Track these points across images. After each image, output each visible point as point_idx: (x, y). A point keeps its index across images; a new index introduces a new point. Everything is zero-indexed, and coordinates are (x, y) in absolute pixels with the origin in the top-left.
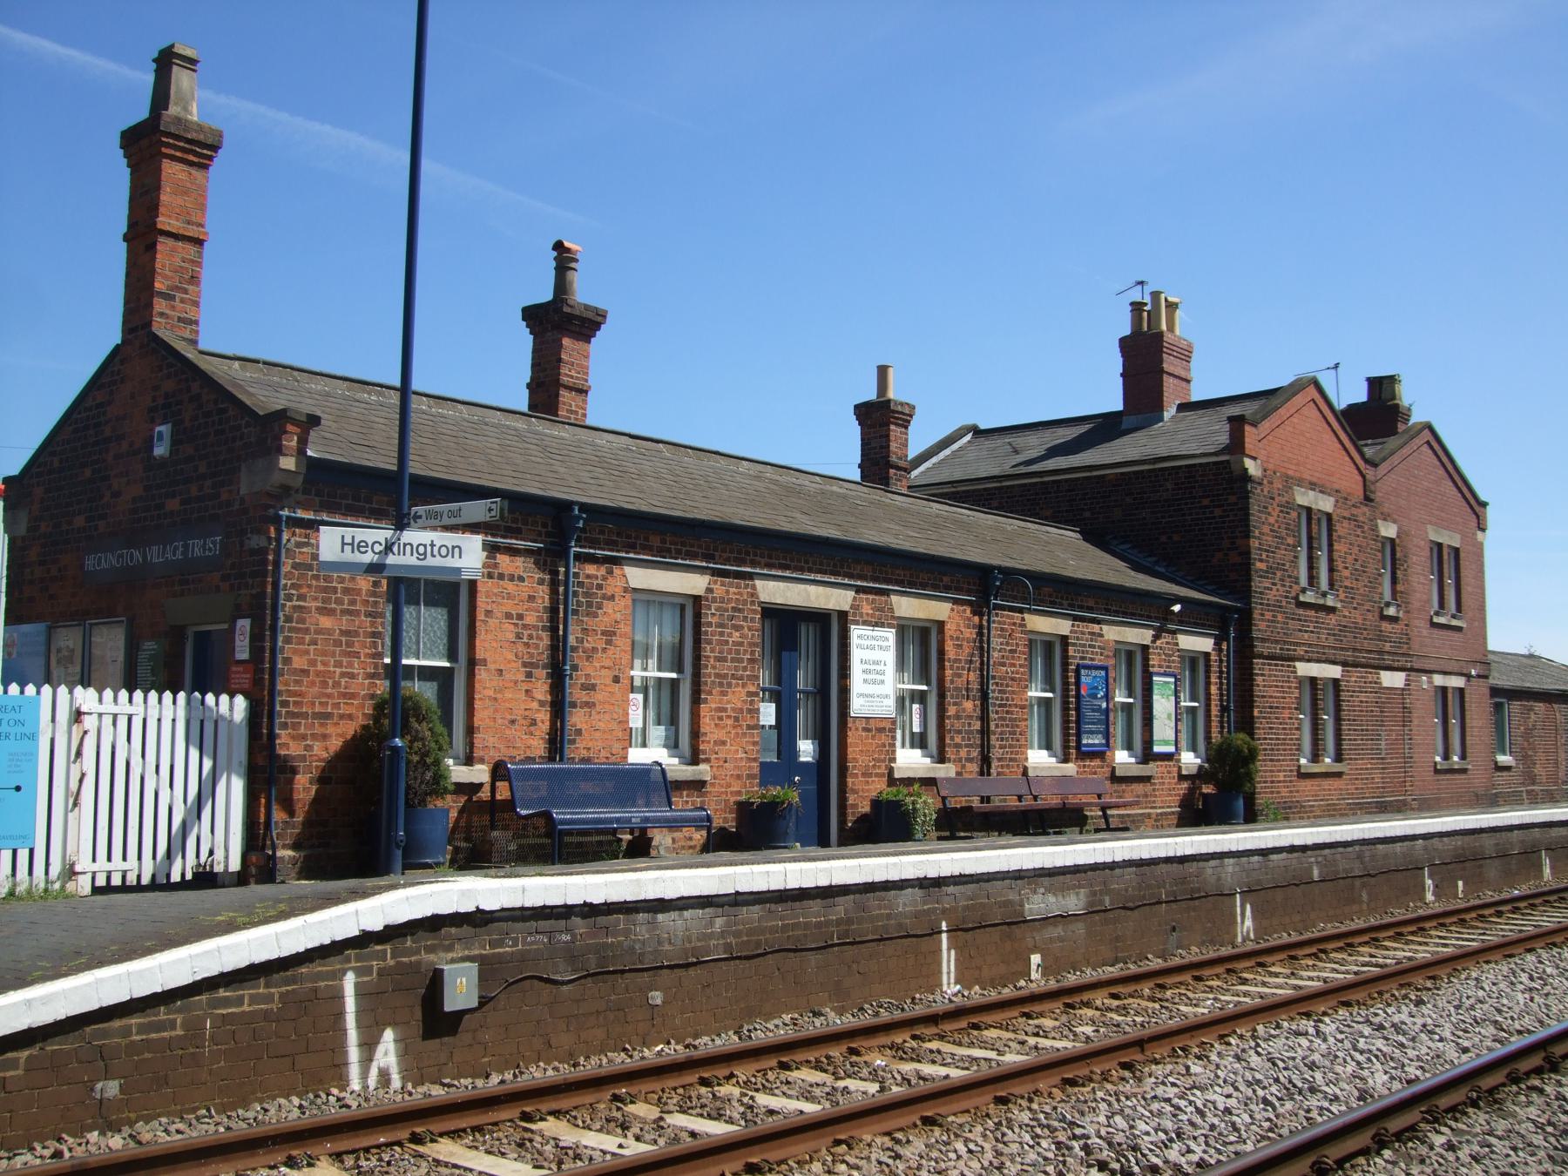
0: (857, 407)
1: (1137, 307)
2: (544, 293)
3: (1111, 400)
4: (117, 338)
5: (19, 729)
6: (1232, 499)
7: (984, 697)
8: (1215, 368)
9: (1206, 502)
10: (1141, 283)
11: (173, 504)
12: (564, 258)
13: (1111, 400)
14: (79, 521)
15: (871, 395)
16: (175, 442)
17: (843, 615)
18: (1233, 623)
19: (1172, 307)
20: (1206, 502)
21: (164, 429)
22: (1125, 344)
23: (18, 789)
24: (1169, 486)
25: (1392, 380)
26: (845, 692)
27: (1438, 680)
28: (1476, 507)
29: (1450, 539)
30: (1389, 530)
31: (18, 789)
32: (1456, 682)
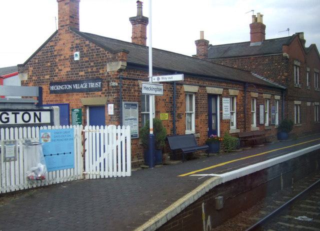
0: (196, 41)
1: (254, 16)
2: (134, 14)
5: (70, 137)
6: (283, 63)
7: (244, 113)
9: (276, 64)
11: (82, 73)
14: (47, 77)
15: (199, 38)
16: (81, 57)
17: (220, 95)
19: (262, 16)
20: (276, 64)
21: (78, 53)
23: (70, 153)
25: (302, 33)
26: (221, 114)
31: (70, 153)
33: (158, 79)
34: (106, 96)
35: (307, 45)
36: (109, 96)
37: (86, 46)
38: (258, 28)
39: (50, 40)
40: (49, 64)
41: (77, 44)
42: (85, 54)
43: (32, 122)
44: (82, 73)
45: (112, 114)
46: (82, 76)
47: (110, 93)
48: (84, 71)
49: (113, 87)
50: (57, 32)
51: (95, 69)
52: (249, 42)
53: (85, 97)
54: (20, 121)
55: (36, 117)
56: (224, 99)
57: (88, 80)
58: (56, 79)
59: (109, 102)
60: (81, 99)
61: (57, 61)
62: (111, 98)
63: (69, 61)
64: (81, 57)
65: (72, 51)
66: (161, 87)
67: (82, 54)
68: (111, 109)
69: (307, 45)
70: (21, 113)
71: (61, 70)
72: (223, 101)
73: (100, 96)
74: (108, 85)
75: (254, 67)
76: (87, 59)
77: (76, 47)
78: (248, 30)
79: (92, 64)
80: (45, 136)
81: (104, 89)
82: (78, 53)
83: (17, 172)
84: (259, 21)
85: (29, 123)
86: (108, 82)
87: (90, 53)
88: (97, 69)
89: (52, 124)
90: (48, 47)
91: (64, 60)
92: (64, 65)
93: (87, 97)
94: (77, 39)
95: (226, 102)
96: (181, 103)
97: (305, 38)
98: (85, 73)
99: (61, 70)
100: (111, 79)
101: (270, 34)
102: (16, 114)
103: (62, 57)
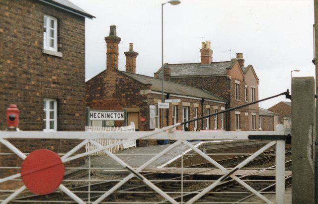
1: (204, 43)
10: (203, 37)
12: (131, 45)
19: (210, 43)
22: (202, 51)
24: (215, 80)
25: (241, 54)
27: (253, 114)
28: (257, 80)
29: (254, 87)
30: (246, 86)
32: (255, 114)
38: (206, 52)
39: (100, 74)
50: (105, 70)
51: (132, 93)
61: (106, 86)
66: (168, 104)
69: (246, 65)
75: (205, 84)
76: (127, 87)
78: (200, 54)
79: (131, 90)
84: (208, 47)
101: (216, 58)
103: (109, 85)
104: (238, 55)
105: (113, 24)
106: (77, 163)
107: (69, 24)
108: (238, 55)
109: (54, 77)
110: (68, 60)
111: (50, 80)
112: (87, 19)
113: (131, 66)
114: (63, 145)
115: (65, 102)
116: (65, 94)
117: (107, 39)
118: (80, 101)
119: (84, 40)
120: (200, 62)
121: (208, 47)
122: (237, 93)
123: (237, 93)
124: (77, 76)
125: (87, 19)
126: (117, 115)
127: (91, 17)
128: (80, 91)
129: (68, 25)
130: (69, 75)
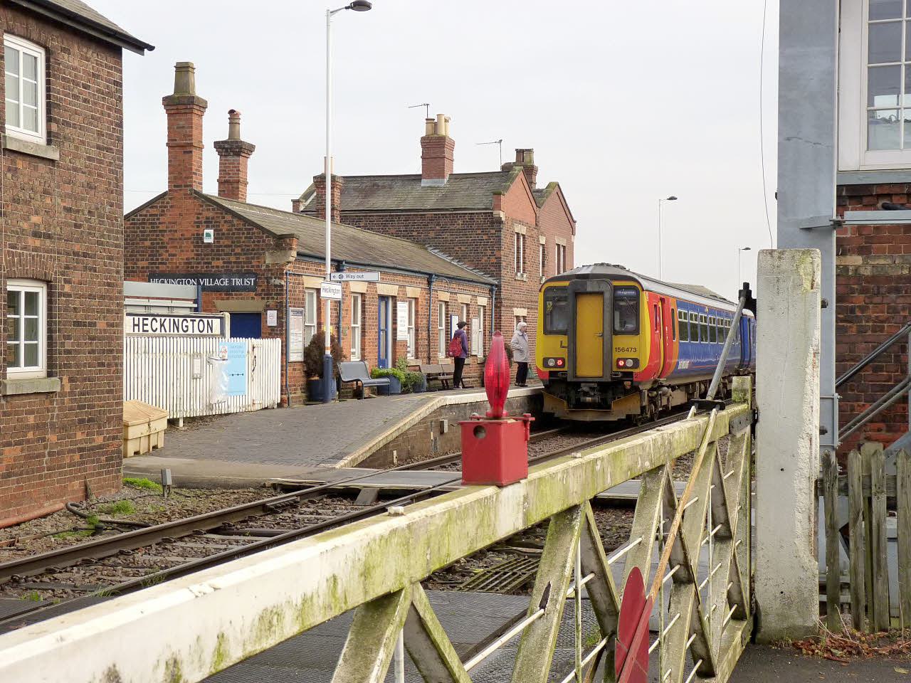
3: (416, 168)
4: (163, 187)
6: (493, 231)
8: (470, 158)
9: (479, 232)
11: (220, 263)
13: (416, 168)
14: (145, 264)
17: (394, 297)
18: (495, 291)
20: (479, 232)
21: (211, 232)
24: (460, 222)
26: (395, 330)
28: (572, 222)
29: (563, 242)
30: (543, 241)
33: (341, 277)
34: (263, 298)
35: (541, 182)
36: (268, 298)
37: (225, 222)
38: (435, 147)
40: (148, 243)
41: (207, 218)
42: (223, 234)
43: (205, 332)
44: (220, 263)
45: (275, 324)
46: (217, 267)
47: (271, 294)
48: (223, 259)
49: (276, 286)
50: (165, 194)
52: (417, 178)
53: (223, 299)
54: (197, 332)
55: (163, 328)
56: (399, 304)
57: (230, 274)
58: (163, 268)
59: (268, 308)
60: (215, 301)
61: (166, 239)
62: (271, 302)
63: (193, 243)
64: (215, 238)
65: (198, 227)
67: (218, 234)
68: (272, 318)
69: (541, 182)
70: (198, 320)
71: (174, 255)
72: (398, 308)
73: (253, 298)
74: (268, 282)
75: (432, 235)
76: (227, 242)
77: (205, 222)
78: (419, 150)
79: (238, 250)
80: (223, 350)
81: (259, 289)
82: (211, 232)
83: (201, 394)
85: (187, 333)
86: (268, 279)
87: (234, 234)
88: (247, 258)
89: (223, 334)
90: (146, 215)
91: (180, 239)
92: (181, 247)
93: (228, 299)
94: (208, 210)
95: (403, 309)
96: (347, 310)
97: (536, 164)
98: (224, 263)
99: (174, 255)
100: (272, 274)
102: (193, 321)
103: (178, 235)
104: (520, 153)
105: (183, 59)
106: (98, 461)
107: (76, 64)
108: (520, 153)
109: (35, 219)
110: (75, 169)
111: (25, 226)
112: (127, 53)
113: (231, 183)
114: (60, 409)
115: (67, 289)
116: (67, 267)
117: (168, 102)
118: (109, 285)
119: (120, 112)
120: (421, 173)
121: (442, 132)
122: (518, 258)
123: (518, 258)
124: (100, 216)
125: (127, 53)
126: (196, 323)
127: (139, 47)
128: (110, 258)
129: (75, 69)
130: (78, 211)
